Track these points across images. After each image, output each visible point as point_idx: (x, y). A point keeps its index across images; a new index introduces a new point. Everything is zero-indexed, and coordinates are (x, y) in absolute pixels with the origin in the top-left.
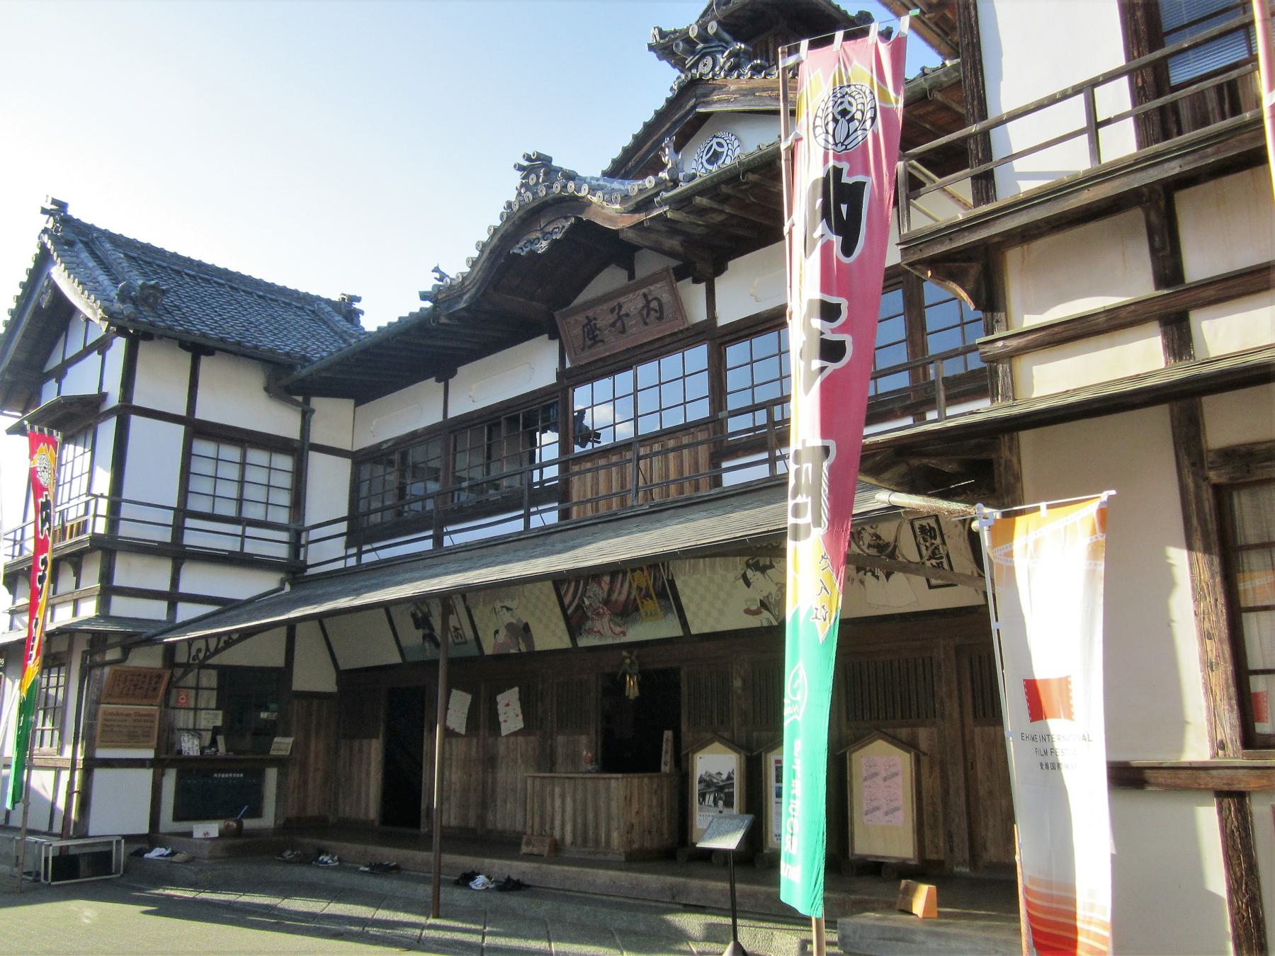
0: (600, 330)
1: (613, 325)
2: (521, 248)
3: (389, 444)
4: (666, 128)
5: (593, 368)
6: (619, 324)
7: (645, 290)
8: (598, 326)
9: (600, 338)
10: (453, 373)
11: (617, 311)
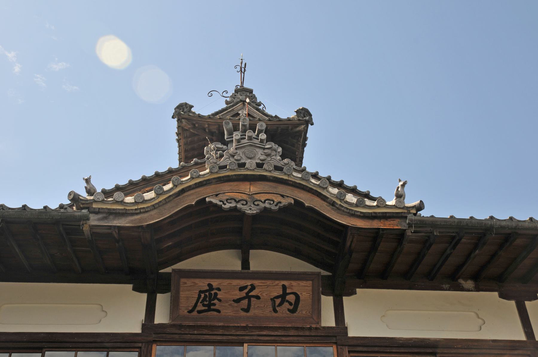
0: (220, 300)
1: (238, 301)
5: (196, 332)
6: (246, 302)
7: (286, 283)
8: (218, 297)
9: (216, 307)
11: (246, 291)
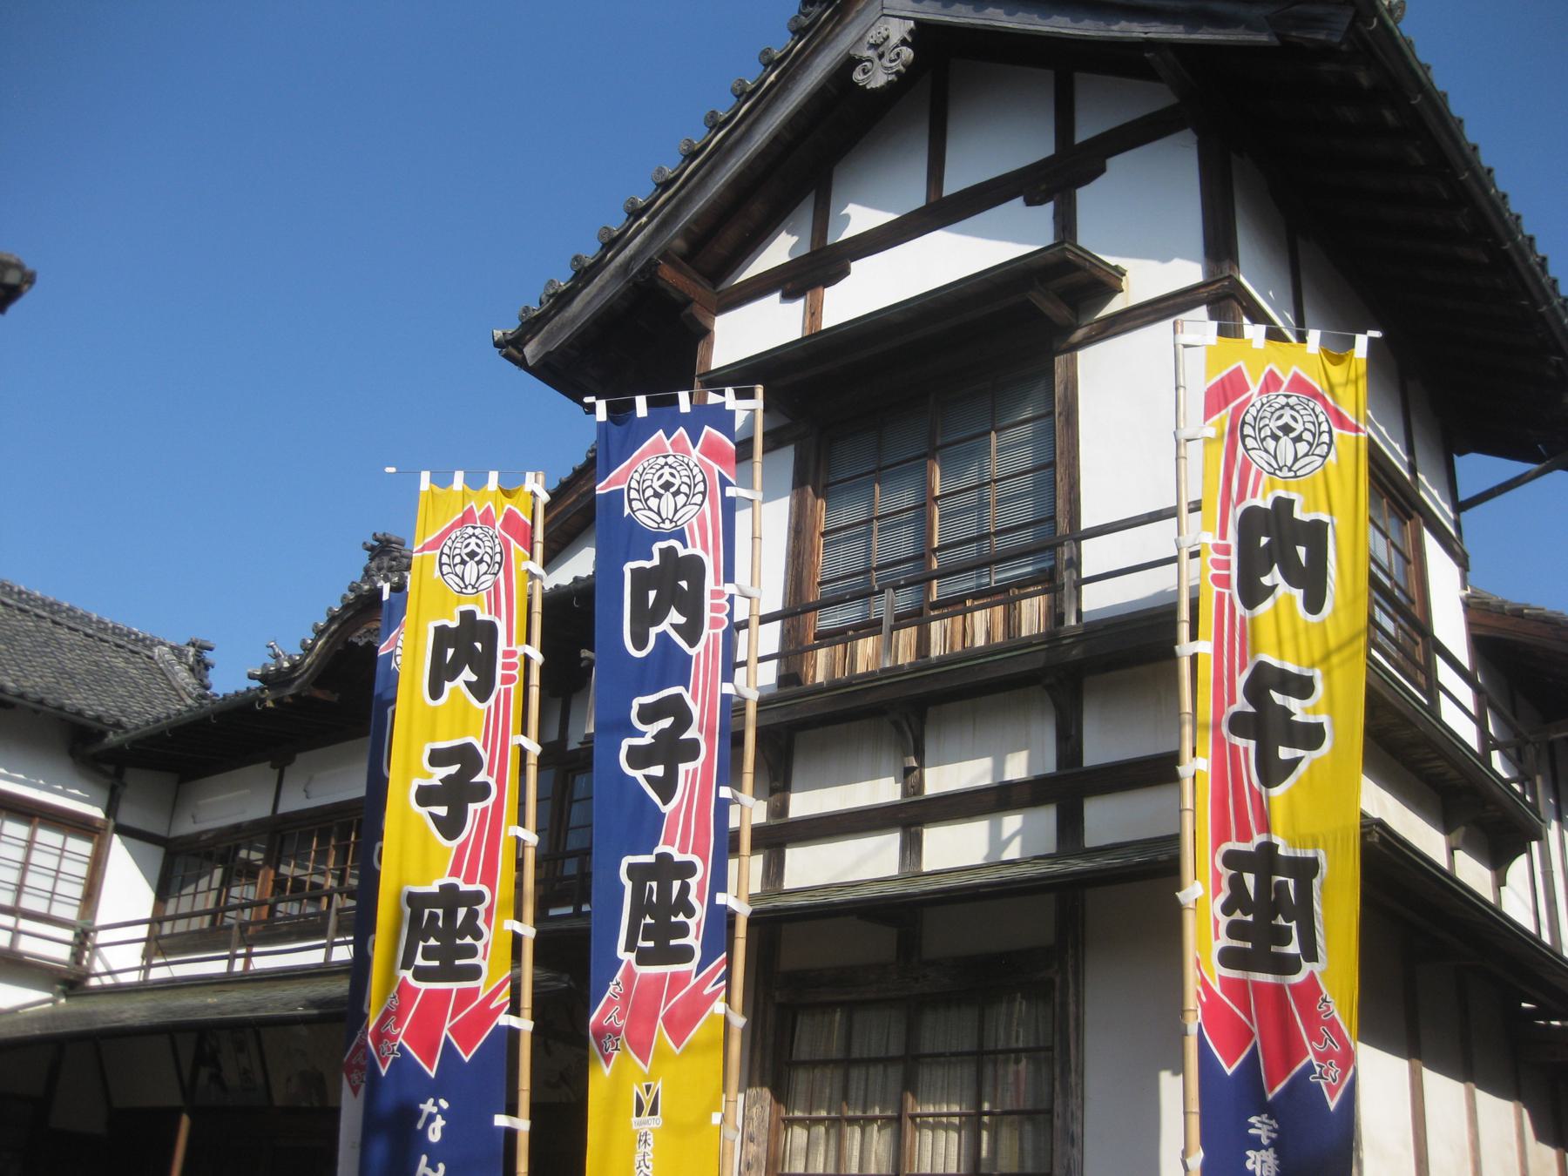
2: (360, 637)
3: (210, 835)
4: (571, 500)
10: (289, 760)
